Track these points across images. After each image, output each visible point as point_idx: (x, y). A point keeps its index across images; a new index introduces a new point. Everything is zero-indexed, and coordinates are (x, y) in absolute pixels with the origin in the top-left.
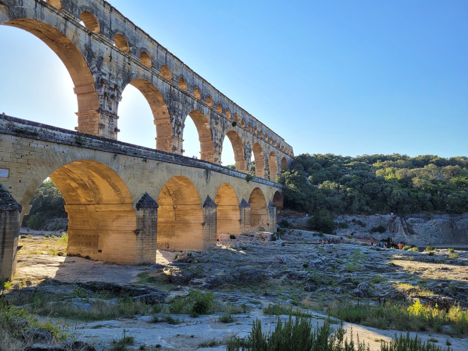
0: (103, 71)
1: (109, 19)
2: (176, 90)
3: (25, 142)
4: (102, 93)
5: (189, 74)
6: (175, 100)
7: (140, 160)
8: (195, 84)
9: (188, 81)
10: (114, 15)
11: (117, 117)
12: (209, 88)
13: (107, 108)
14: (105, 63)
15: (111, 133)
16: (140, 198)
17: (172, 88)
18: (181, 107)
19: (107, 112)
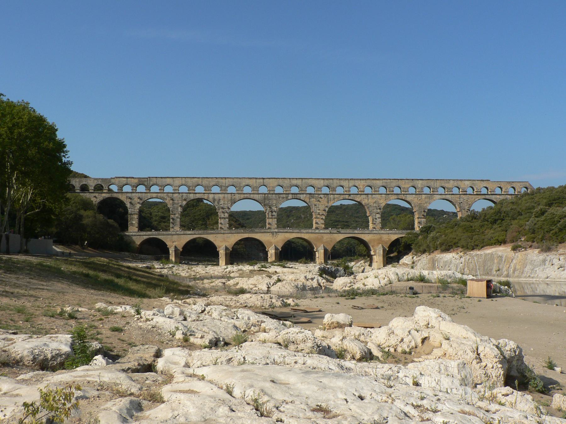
10: (227, 180)
13: (223, 216)
18: (274, 202)
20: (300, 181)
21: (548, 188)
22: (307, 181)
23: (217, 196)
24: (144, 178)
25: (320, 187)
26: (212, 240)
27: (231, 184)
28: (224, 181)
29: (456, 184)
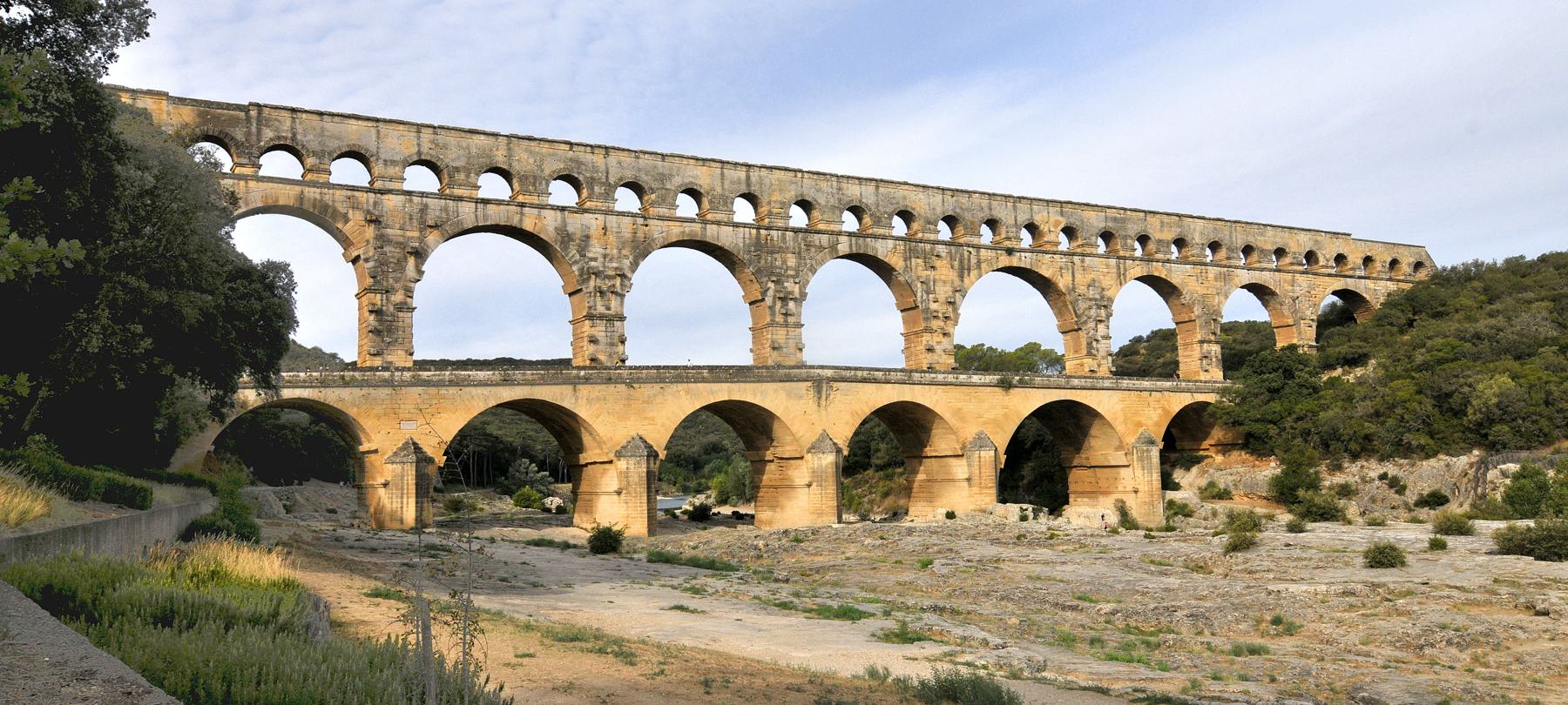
0: (590, 255)
1: (603, 168)
2: (774, 233)
3: (433, 390)
4: (591, 289)
5: (824, 185)
6: (772, 253)
7: (622, 387)
8: (846, 199)
9: (822, 202)
10: (613, 159)
11: (622, 318)
12: (900, 192)
13: (601, 309)
14: (594, 242)
15: (612, 344)
16: (624, 443)
17: (763, 232)
18: (792, 261)
19: (601, 317)
20: (871, 188)
21: (1543, 259)
22: (891, 190)
23: (575, 223)
24: (229, 106)
25: (932, 218)
26: (583, 411)
27: (629, 176)
28: (598, 159)
29: (1279, 240)
